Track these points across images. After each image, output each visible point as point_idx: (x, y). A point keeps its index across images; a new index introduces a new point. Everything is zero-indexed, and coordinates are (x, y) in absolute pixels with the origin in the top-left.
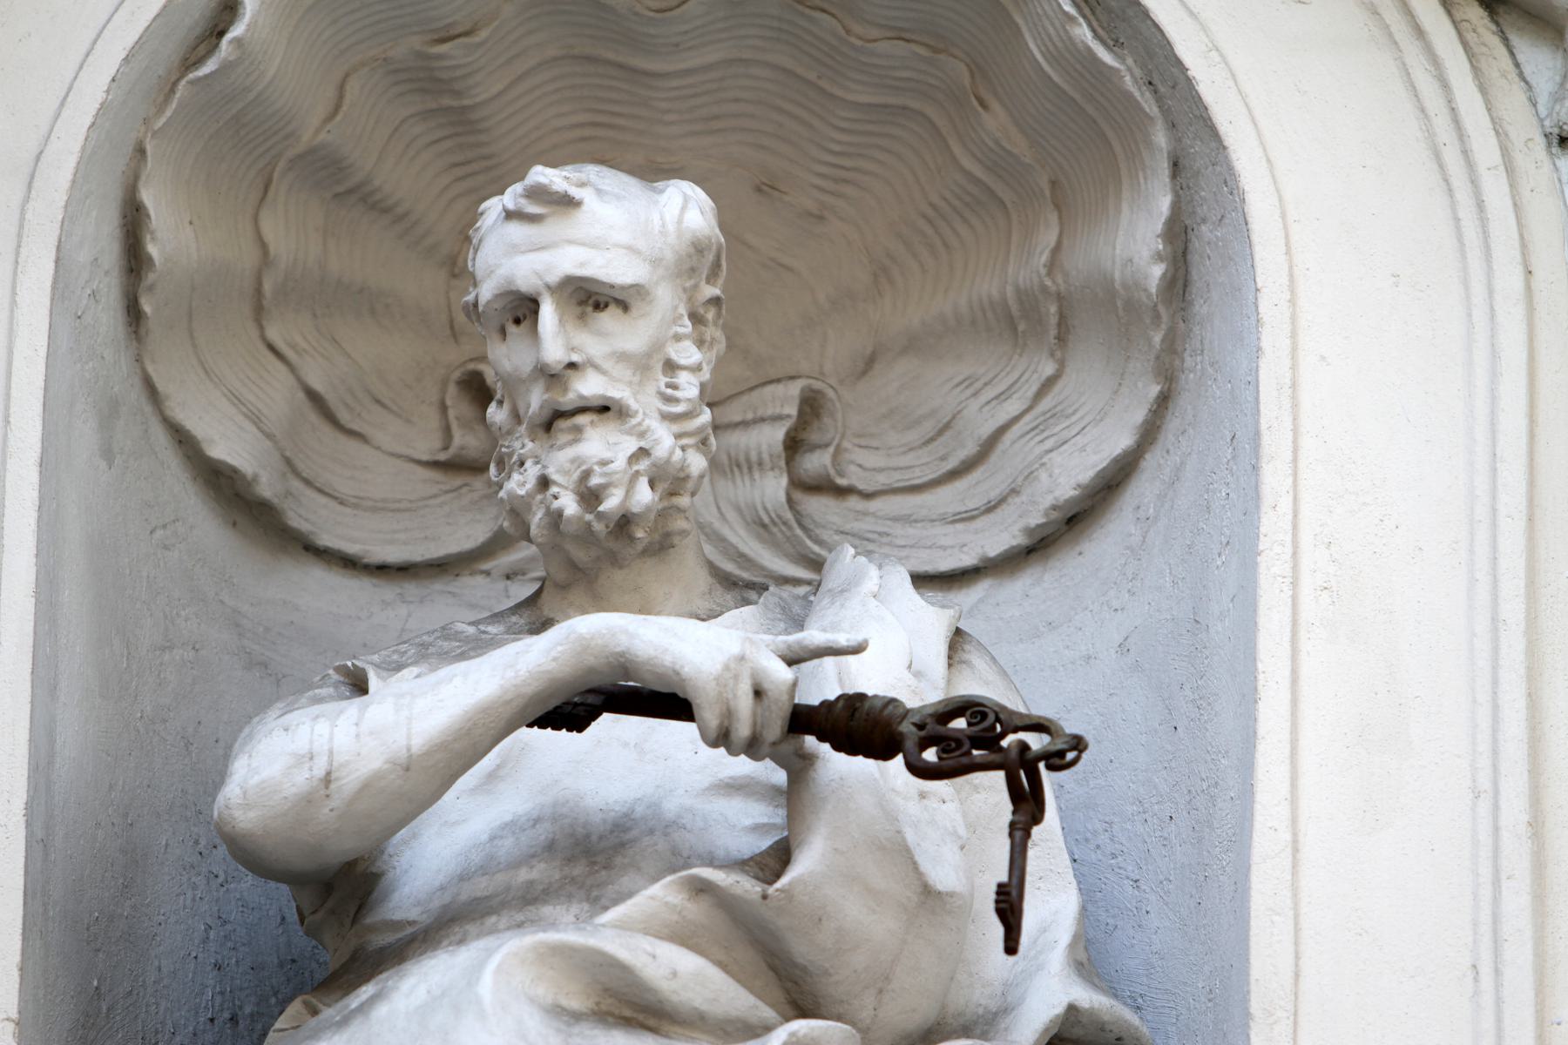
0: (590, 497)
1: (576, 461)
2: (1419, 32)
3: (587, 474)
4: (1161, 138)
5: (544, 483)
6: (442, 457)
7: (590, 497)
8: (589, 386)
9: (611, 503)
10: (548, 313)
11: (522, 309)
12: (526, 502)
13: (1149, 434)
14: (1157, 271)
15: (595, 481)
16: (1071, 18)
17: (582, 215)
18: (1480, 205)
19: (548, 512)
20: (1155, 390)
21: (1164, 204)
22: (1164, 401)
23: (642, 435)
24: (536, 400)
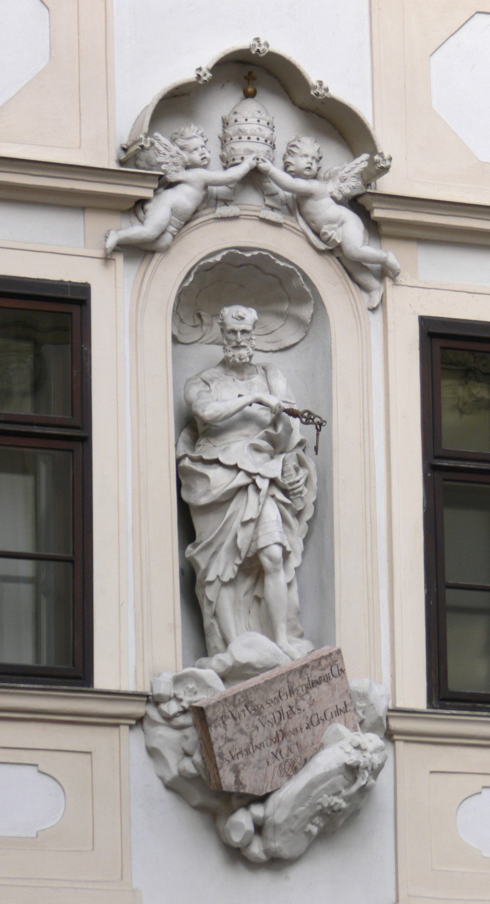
0: (240, 359)
1: (240, 354)
2: (352, 292)
3: (240, 356)
4: (313, 302)
5: (234, 356)
6: (193, 325)
7: (240, 359)
8: (243, 344)
9: (244, 361)
10: (239, 334)
11: (234, 332)
12: (230, 358)
13: (302, 340)
14: (309, 320)
15: (242, 357)
16: (303, 285)
17: (245, 320)
18: (360, 322)
19: (234, 360)
20: (304, 335)
21: (312, 311)
22: (305, 336)
23: (248, 350)
24: (234, 344)
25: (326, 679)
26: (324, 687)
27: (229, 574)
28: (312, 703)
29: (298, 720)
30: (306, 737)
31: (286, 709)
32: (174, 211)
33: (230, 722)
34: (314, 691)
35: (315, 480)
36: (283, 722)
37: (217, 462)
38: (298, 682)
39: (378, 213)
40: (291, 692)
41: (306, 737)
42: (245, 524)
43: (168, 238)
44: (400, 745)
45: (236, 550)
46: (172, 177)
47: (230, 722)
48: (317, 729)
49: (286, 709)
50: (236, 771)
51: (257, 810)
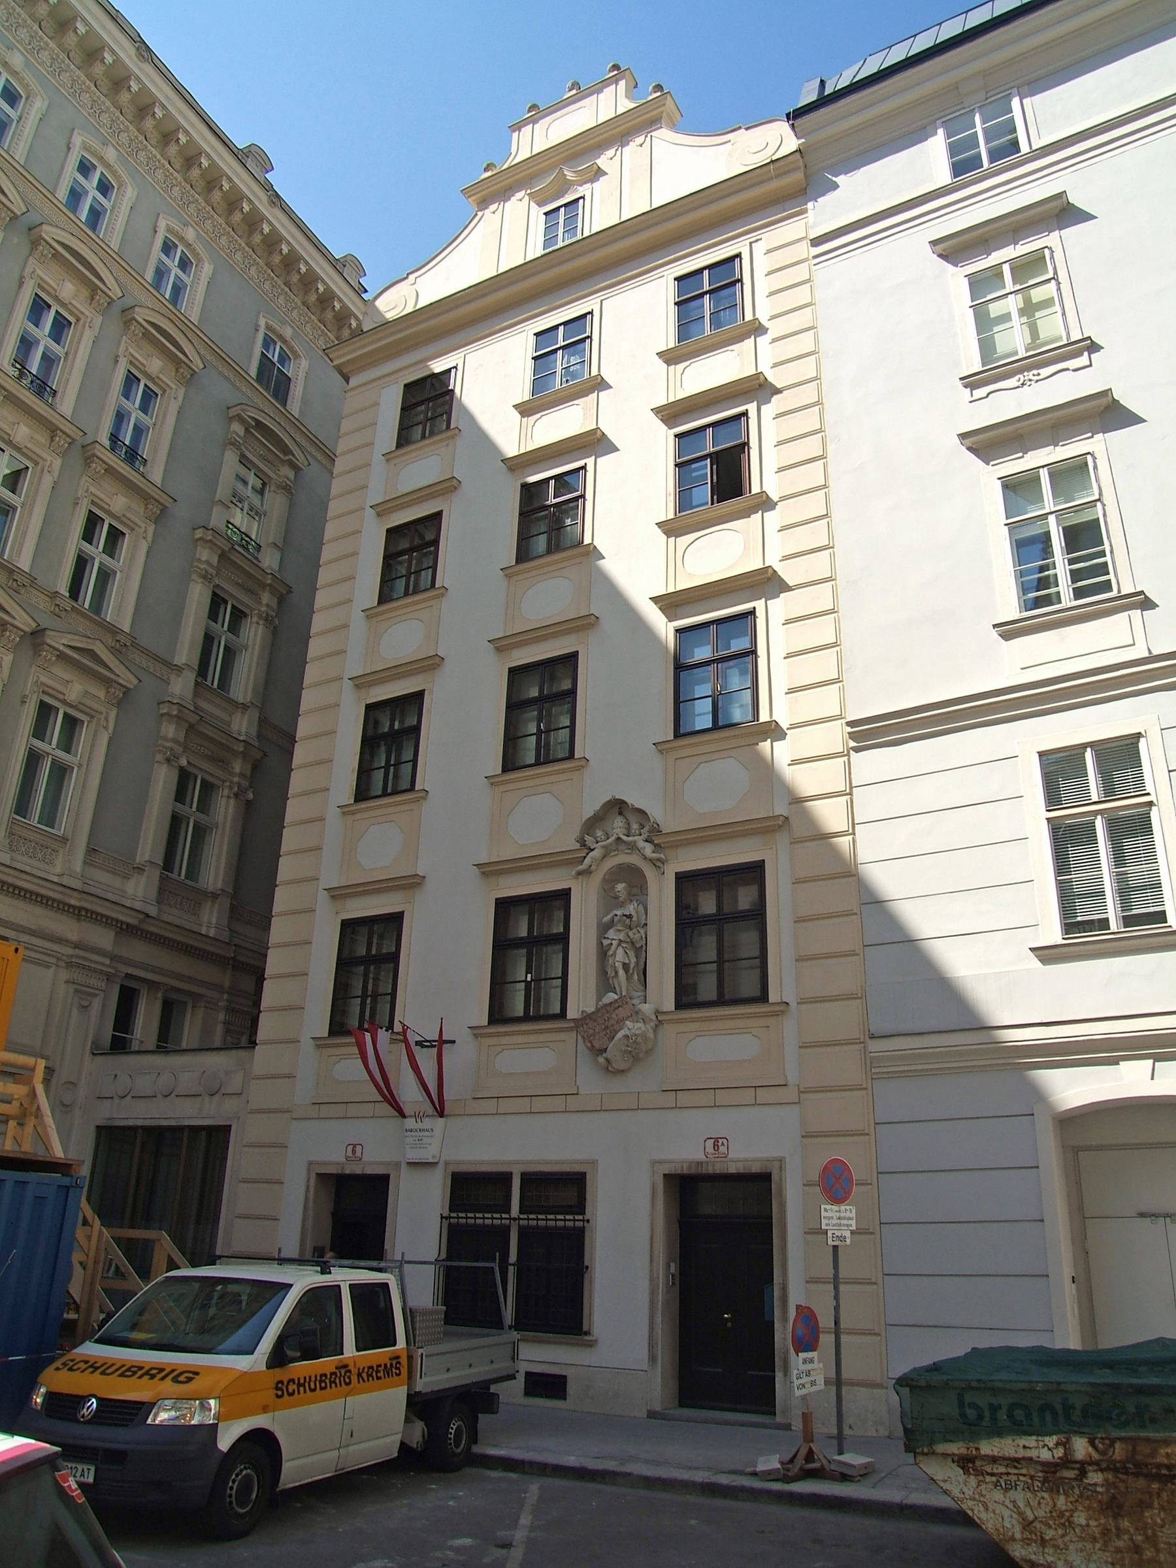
25: (622, 1006)
26: (620, 1009)
27: (613, 974)
28: (617, 1015)
29: (612, 1022)
30: (616, 1027)
31: (606, 1019)
32: (592, 858)
33: (585, 1026)
34: (617, 1011)
35: (644, 936)
36: (607, 1023)
37: (605, 938)
38: (608, 1008)
39: (656, 842)
40: (608, 1012)
41: (616, 1027)
42: (612, 955)
43: (593, 867)
44: (665, 1025)
45: (612, 966)
46: (592, 848)
47: (585, 1026)
48: (621, 1024)
49: (606, 1019)
50: (590, 1042)
51: (604, 1055)
